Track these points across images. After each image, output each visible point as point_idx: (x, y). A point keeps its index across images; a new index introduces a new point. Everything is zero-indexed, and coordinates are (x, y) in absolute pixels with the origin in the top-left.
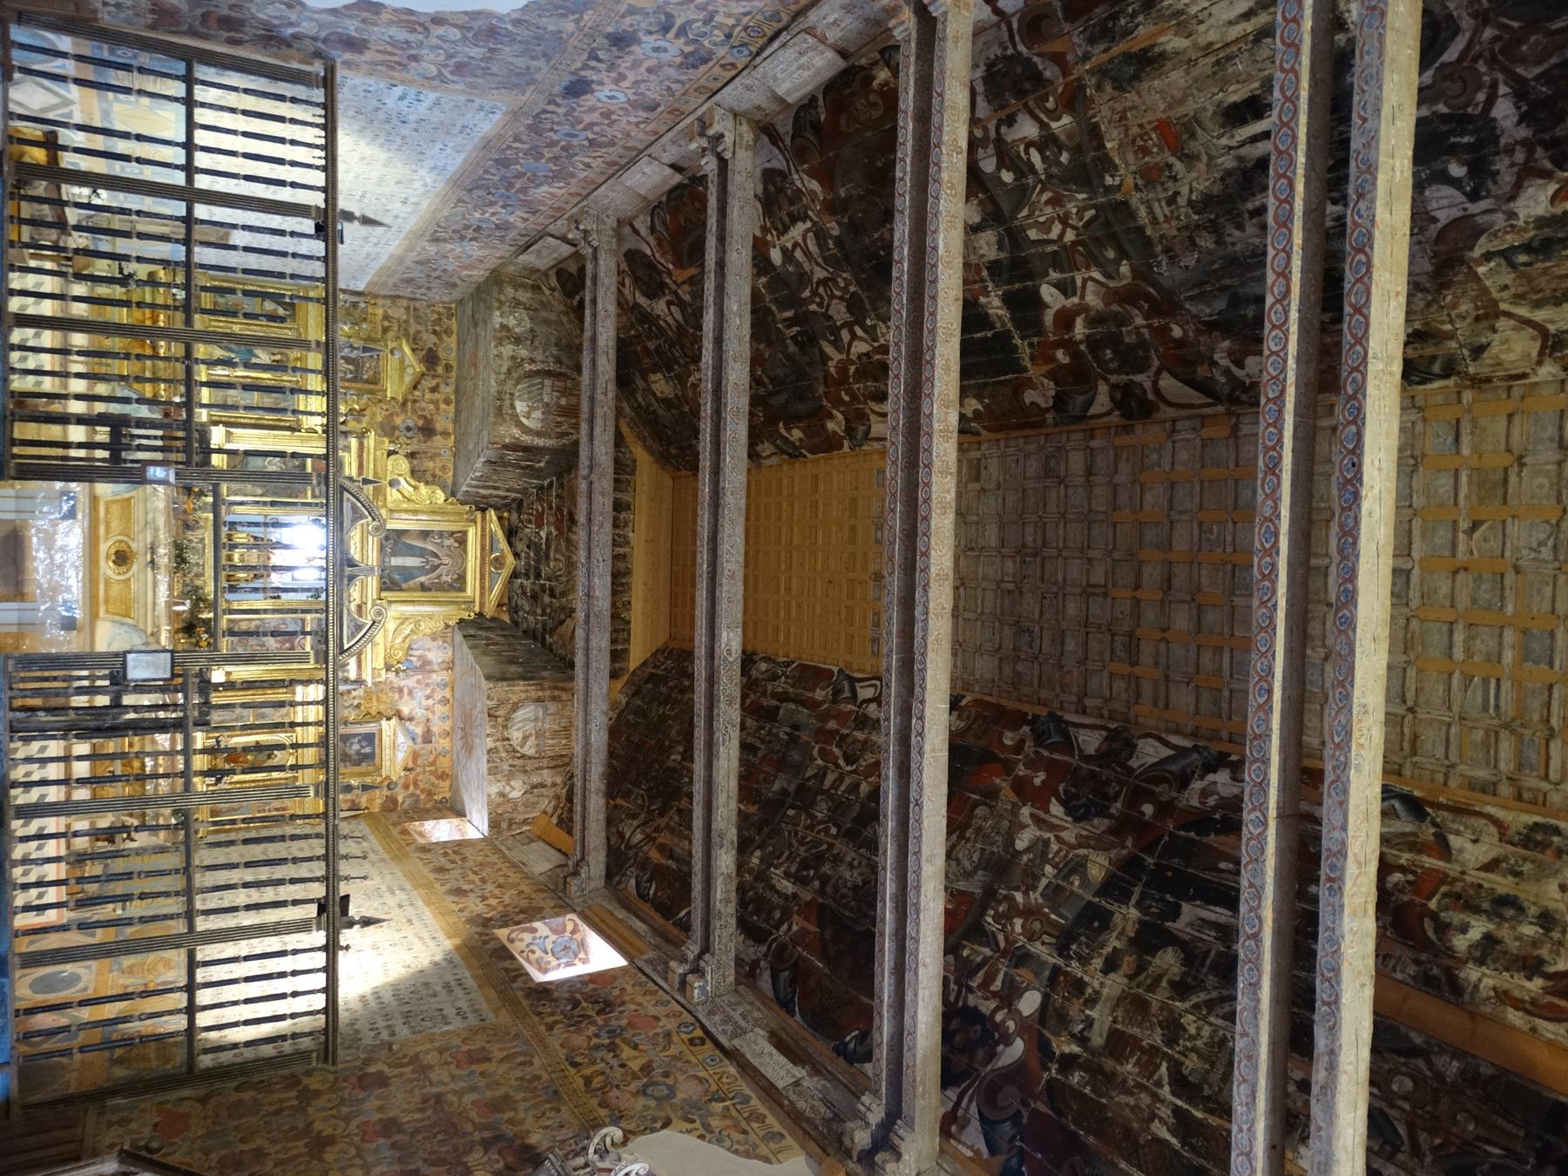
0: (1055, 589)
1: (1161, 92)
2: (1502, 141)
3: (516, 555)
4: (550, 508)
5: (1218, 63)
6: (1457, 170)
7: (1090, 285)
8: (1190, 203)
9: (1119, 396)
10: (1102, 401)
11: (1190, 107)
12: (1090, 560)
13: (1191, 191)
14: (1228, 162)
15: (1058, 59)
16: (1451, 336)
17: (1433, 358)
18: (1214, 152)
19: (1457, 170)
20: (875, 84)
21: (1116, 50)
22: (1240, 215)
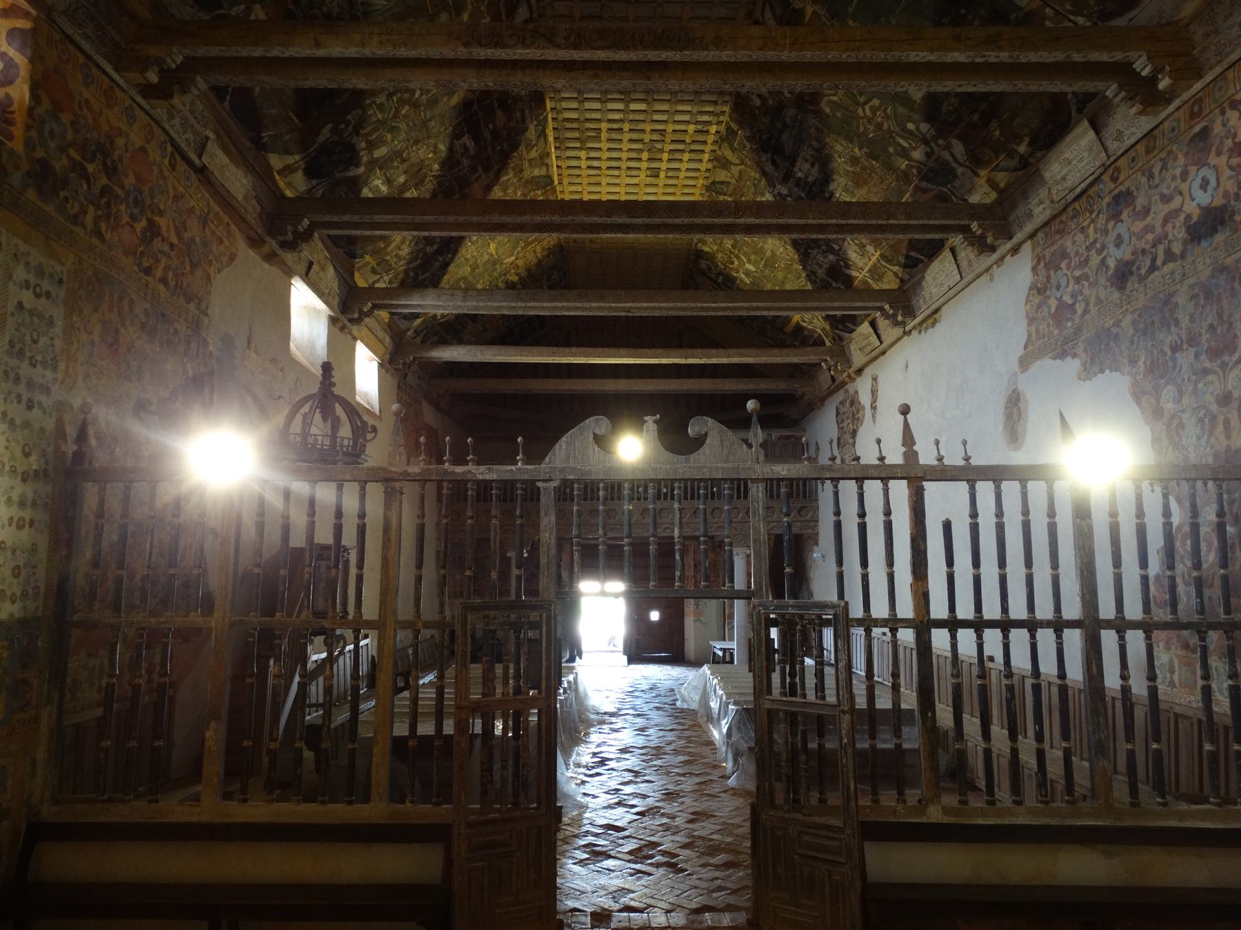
15: (924, 191)
20: (1027, 140)
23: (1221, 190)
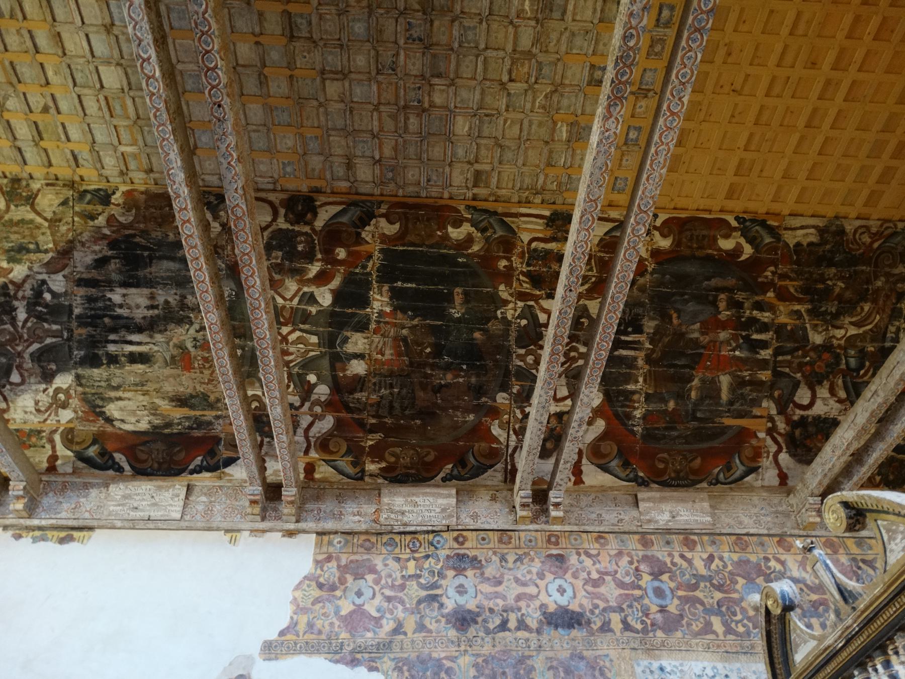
0: (380, 78)
1: (181, 384)
2: (25, 303)
5: (143, 385)
6: (47, 296)
7: (288, 295)
8: (191, 323)
9: (309, 216)
10: (323, 217)
11: (168, 371)
12: (342, 101)
13: (188, 330)
14: (159, 337)
16: (75, 213)
17: (88, 203)
18: (165, 345)
19: (47, 296)
20: (384, 465)
21: (198, 413)
22: (164, 308)
23: (577, 601)
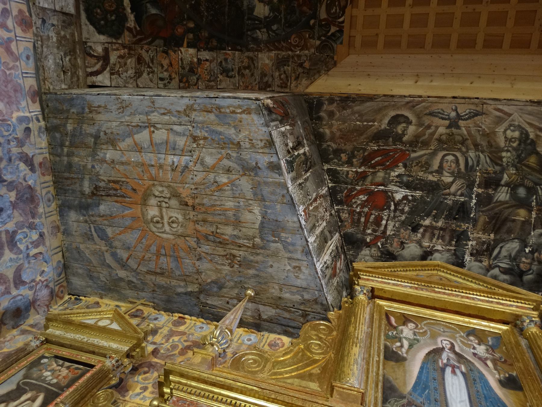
3: (426, 255)
4: (363, 176)
